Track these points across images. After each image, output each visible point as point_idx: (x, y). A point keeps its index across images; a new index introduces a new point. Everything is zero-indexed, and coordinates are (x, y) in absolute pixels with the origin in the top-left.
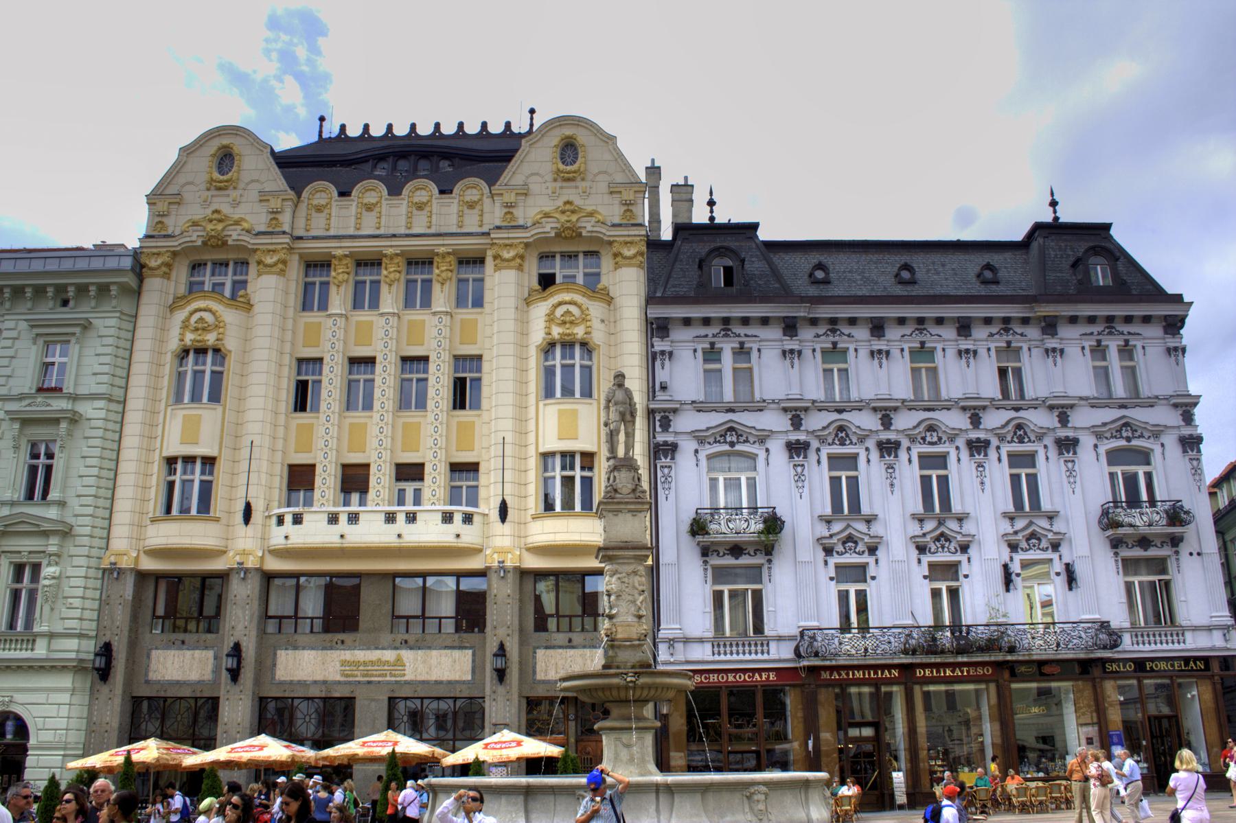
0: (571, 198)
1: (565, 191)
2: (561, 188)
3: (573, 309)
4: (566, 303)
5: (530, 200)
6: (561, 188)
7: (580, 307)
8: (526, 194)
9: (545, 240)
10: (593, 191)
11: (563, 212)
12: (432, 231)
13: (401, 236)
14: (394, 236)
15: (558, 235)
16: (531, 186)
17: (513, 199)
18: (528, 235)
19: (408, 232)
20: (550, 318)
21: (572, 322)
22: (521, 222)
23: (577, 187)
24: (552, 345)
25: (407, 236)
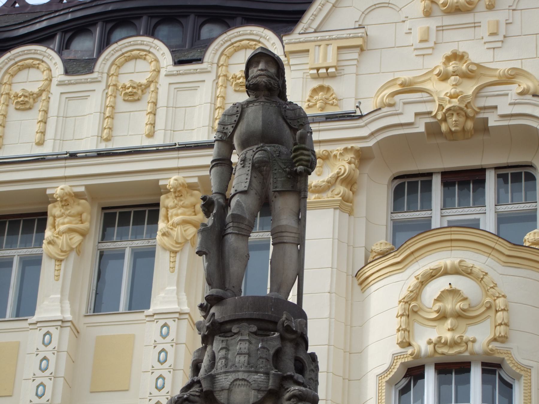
0: (461, 50)
1: (449, 35)
2: (440, 29)
3: (460, 283)
4: (446, 273)
5: (371, 62)
6: (440, 29)
7: (479, 278)
8: (361, 49)
9: (398, 144)
10: (514, 30)
11: (444, 77)
12: (158, 140)
13: (88, 155)
14: (73, 156)
15: (433, 130)
16: (372, 31)
17: (331, 60)
18: (365, 132)
19: (103, 146)
20: (411, 309)
21: (459, 316)
22: (348, 107)
23: (476, 25)
24: (414, 373)
25: (100, 154)
